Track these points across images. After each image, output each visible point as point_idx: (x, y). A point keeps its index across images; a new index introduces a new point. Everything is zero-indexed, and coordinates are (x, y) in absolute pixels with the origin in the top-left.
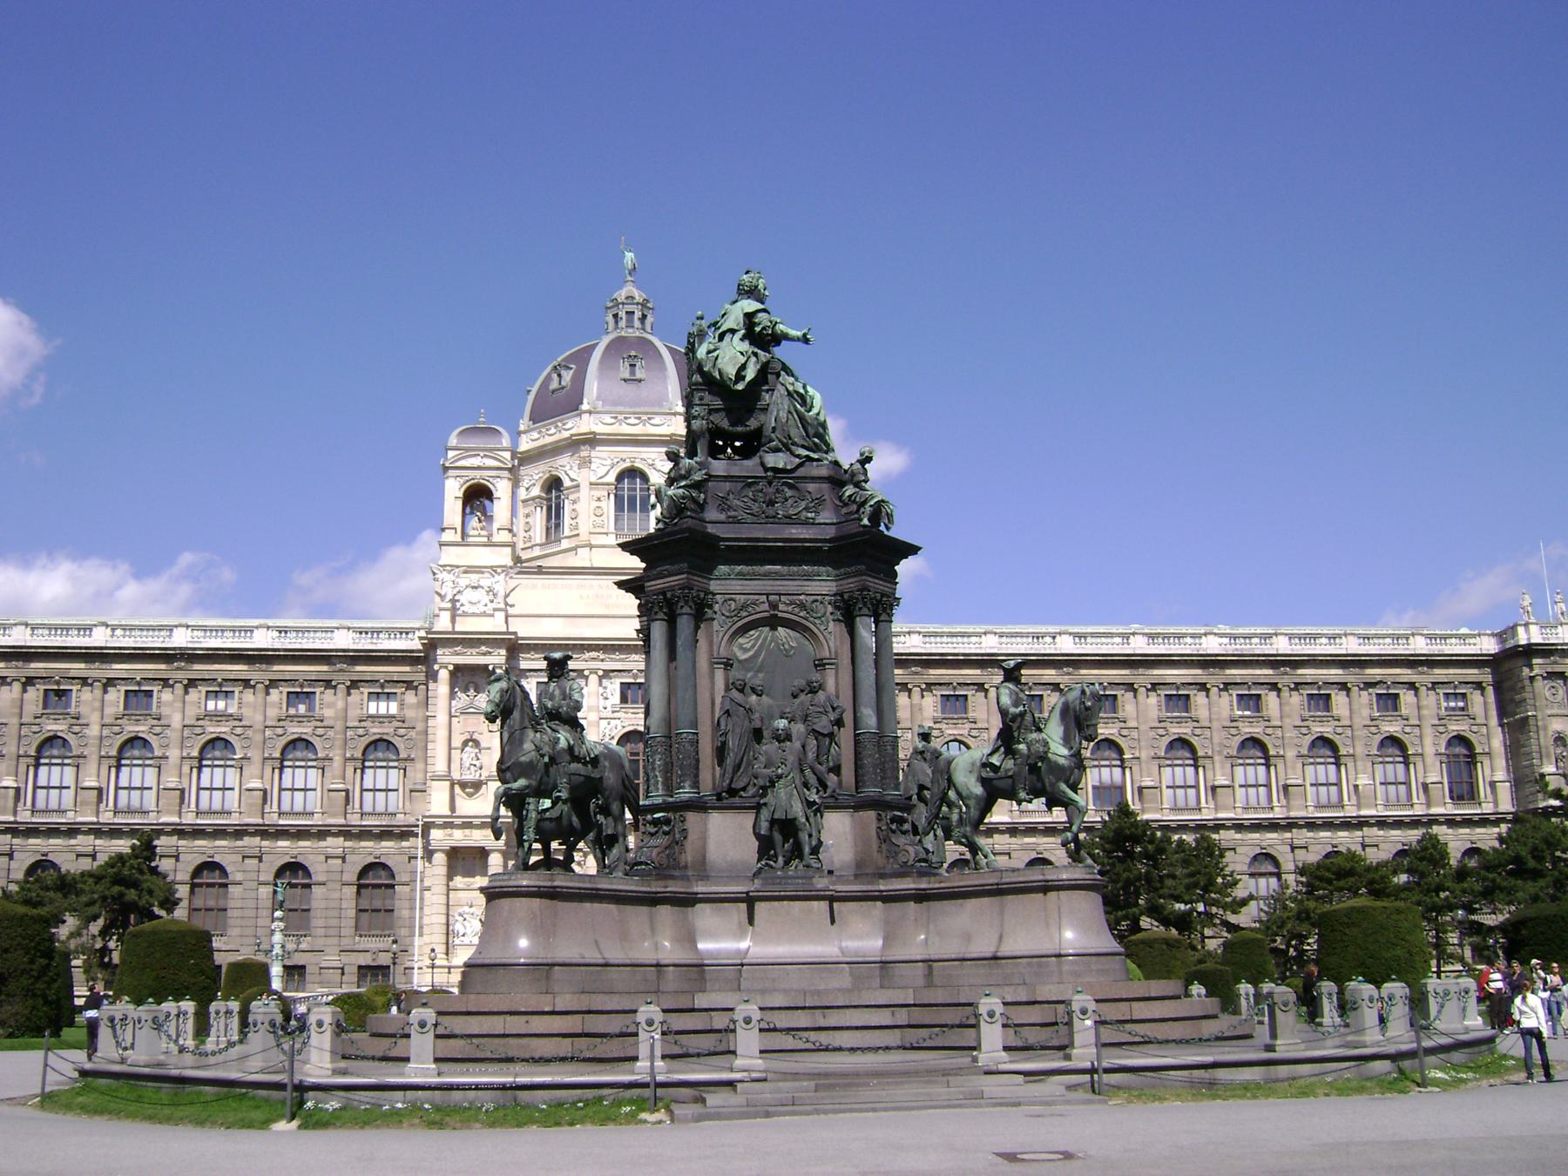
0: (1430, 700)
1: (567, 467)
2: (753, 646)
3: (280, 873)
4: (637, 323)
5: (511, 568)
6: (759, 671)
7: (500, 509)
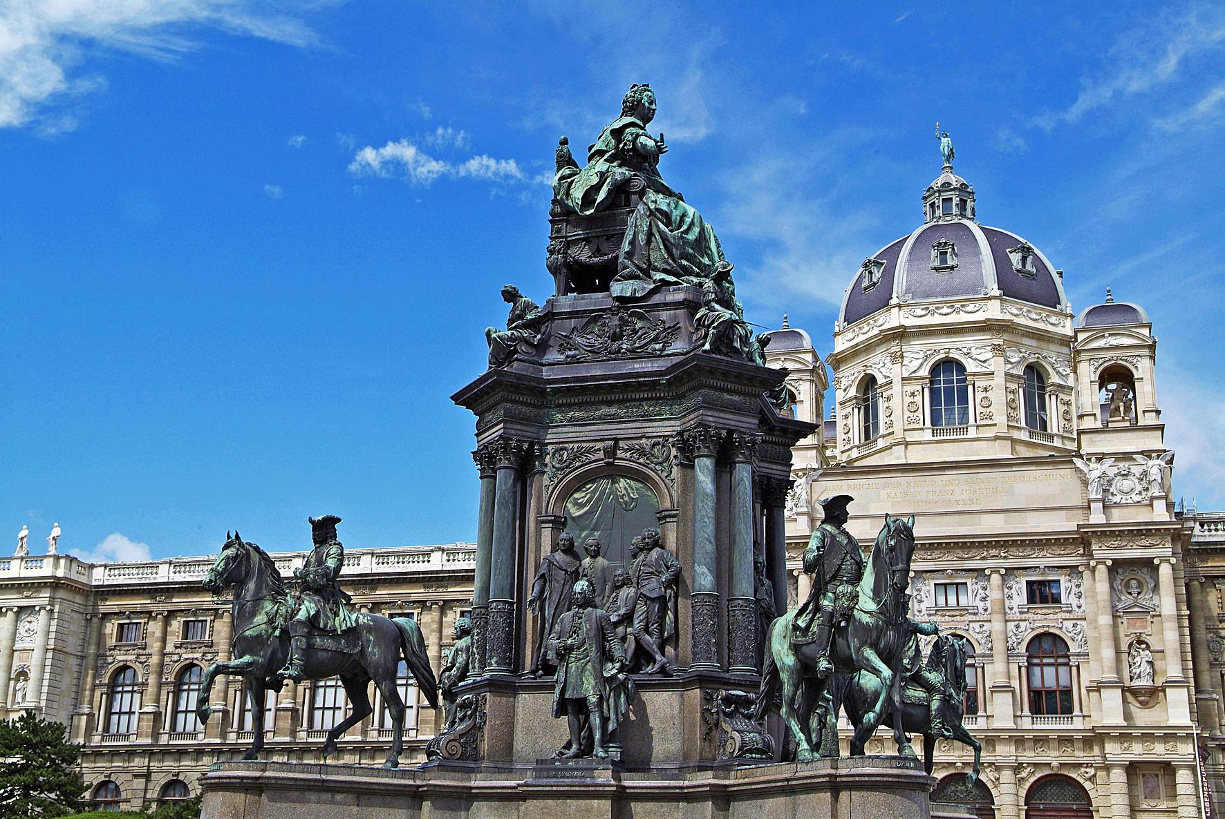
1: (881, 365)
2: (588, 501)
4: (955, 210)
5: (815, 470)
6: (595, 529)
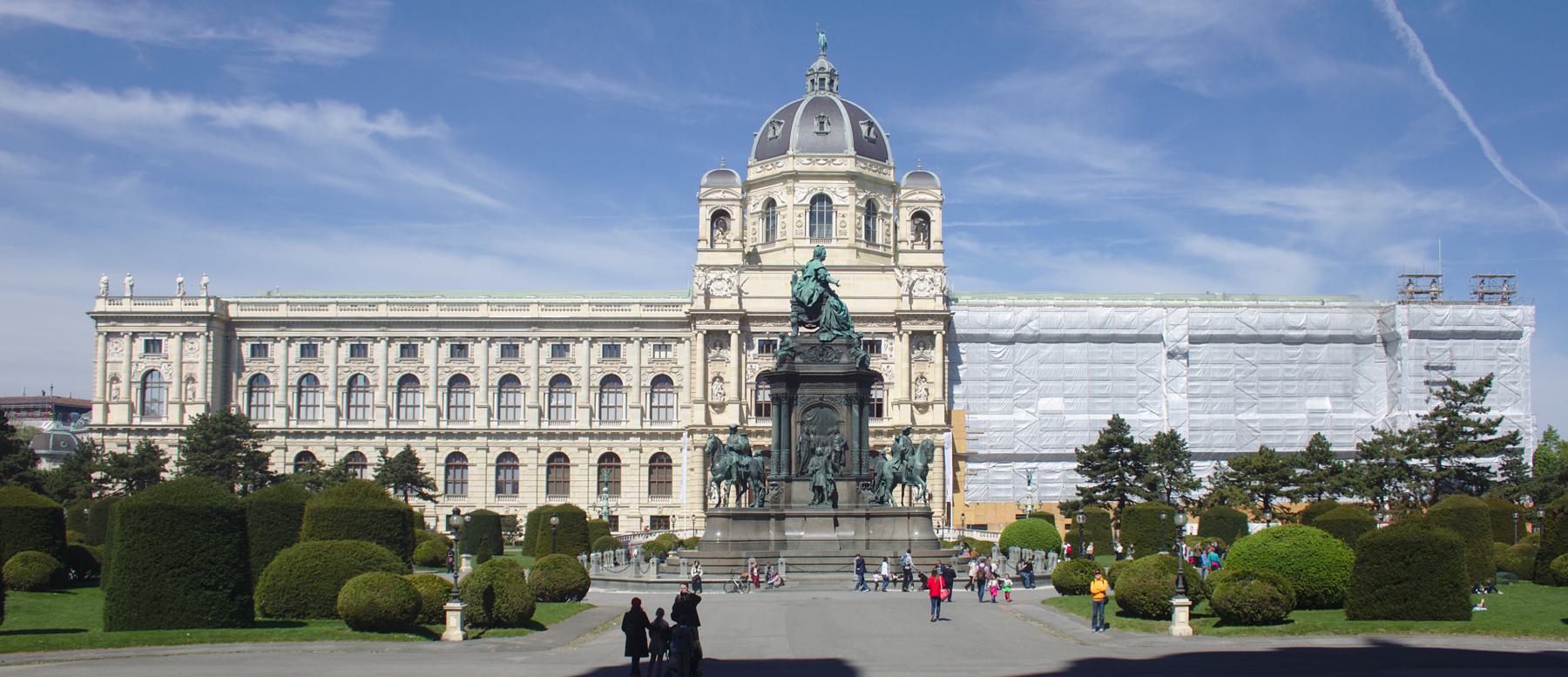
1: (779, 192)
3: (602, 459)
4: (827, 87)
6: (815, 425)
7: (735, 226)
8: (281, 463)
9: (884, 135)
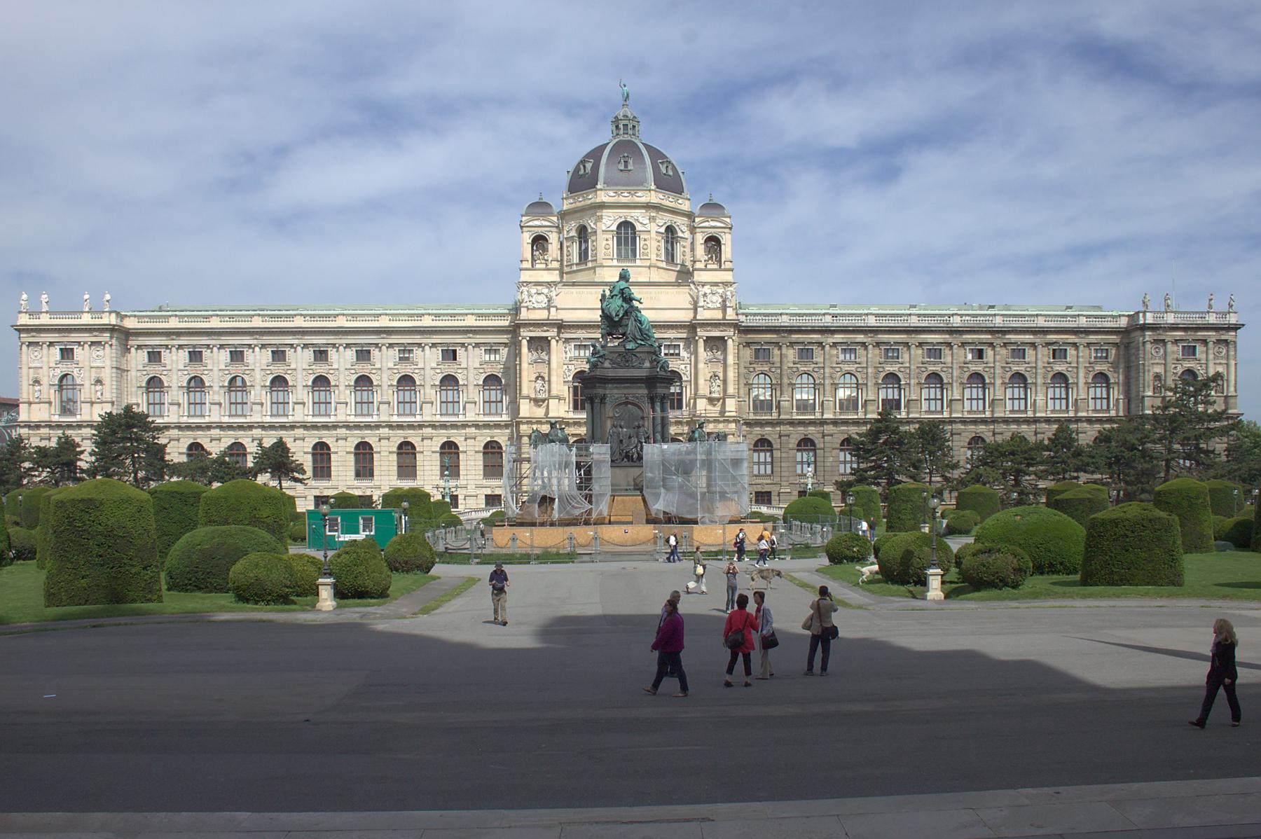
0: (1083, 352)
8: (176, 453)
9: (680, 172)
